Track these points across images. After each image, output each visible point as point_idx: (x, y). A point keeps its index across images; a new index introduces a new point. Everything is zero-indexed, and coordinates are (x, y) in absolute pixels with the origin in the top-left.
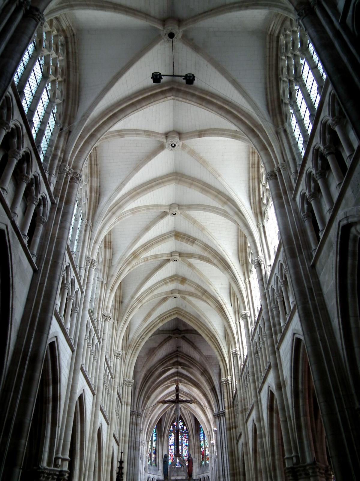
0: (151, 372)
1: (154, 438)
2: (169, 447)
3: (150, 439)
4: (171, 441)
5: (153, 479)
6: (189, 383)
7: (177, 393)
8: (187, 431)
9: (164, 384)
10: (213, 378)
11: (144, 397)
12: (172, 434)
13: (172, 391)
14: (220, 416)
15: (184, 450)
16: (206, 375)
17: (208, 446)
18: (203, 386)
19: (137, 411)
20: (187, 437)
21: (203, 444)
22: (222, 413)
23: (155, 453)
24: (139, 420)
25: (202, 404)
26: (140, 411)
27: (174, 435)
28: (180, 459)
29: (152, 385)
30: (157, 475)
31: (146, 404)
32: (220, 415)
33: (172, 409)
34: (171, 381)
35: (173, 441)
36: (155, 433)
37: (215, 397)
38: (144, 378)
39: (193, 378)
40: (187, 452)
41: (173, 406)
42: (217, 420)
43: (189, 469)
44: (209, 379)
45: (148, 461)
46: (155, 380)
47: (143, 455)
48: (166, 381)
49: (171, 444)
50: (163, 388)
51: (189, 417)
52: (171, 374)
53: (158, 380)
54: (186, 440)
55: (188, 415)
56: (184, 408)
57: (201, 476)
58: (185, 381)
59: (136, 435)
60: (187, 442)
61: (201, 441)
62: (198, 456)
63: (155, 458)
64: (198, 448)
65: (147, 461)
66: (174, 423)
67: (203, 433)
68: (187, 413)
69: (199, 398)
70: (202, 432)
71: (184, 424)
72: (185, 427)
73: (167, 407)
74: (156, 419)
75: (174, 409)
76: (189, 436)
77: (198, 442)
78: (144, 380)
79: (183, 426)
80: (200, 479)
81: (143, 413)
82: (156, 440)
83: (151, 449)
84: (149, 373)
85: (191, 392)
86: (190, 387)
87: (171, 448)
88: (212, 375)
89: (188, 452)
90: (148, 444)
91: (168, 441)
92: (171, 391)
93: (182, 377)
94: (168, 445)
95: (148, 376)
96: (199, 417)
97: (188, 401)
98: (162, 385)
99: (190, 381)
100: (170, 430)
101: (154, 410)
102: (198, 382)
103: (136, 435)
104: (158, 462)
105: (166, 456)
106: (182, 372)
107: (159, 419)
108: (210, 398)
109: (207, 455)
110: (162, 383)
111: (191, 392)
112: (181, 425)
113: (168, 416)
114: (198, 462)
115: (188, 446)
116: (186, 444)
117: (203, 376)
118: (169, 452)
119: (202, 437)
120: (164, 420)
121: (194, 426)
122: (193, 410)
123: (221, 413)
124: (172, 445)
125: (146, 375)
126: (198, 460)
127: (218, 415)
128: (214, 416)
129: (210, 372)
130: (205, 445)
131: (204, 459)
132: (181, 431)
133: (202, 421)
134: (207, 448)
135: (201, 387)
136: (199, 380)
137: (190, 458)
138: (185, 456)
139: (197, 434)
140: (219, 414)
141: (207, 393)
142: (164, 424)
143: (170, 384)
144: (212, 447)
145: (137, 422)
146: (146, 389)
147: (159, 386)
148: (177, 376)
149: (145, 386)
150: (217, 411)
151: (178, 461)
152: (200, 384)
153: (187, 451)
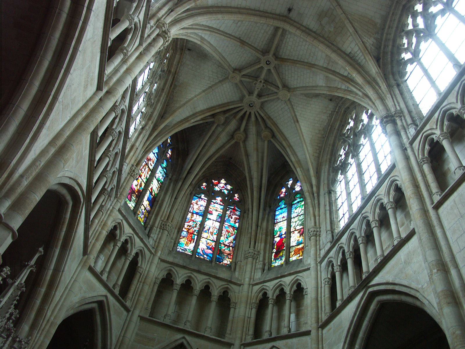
4: (196, 207)
15: (224, 232)
30: (141, 240)
35: (202, 208)
40: (231, 239)
49: (196, 210)
54: (234, 217)
60: (235, 222)
87: (193, 219)
89: (234, 239)
91: (189, 203)
94: (186, 211)
100: (200, 188)
115: (237, 229)
116: (232, 223)
118: (186, 224)
138: (225, 245)
142: (189, 163)
153: (233, 237)
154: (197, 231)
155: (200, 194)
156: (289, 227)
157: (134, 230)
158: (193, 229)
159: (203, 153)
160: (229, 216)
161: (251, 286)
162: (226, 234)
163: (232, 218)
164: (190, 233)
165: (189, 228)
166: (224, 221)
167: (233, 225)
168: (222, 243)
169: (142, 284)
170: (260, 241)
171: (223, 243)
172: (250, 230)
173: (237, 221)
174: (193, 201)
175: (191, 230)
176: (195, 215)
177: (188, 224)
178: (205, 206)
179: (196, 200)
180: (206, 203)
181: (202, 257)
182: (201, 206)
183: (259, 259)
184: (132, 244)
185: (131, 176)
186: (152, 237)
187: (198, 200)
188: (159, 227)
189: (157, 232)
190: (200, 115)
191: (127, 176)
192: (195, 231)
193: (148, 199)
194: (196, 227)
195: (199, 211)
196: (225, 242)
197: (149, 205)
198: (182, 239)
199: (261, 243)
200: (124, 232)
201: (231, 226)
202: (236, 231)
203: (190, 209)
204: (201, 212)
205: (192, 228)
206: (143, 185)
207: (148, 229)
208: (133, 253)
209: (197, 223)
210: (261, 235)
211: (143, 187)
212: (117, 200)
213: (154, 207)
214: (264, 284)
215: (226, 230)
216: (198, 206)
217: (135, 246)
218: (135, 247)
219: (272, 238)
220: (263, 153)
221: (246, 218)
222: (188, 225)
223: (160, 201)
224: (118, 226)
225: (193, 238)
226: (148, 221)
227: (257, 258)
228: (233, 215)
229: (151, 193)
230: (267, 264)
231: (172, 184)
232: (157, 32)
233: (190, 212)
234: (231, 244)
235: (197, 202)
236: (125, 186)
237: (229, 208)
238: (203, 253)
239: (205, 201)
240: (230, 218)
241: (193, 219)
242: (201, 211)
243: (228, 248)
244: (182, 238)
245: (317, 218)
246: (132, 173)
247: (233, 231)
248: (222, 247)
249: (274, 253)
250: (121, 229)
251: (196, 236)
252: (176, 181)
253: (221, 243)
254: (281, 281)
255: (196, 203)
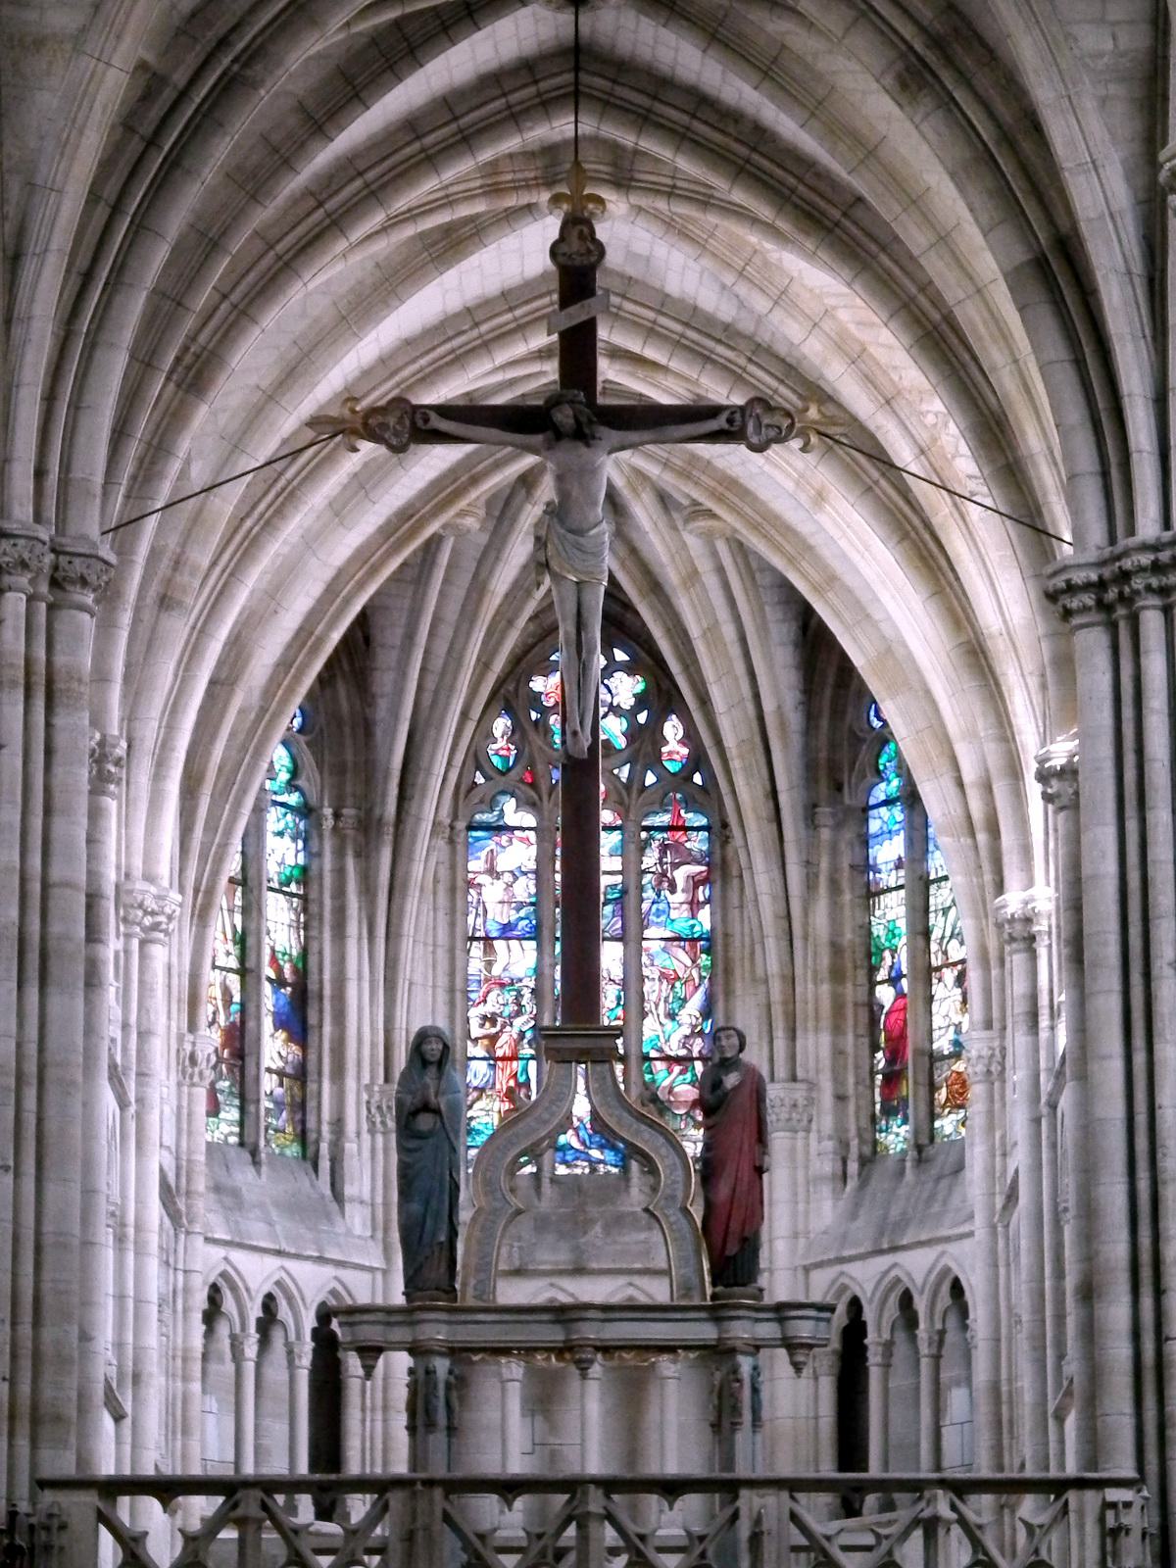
0: (223, 43)
1: (282, 853)
2: (477, 949)
3: (233, 865)
4: (493, 892)
5: (269, 1303)
6: (739, 196)
7: (577, 314)
8: (697, 779)
9: (402, 202)
10: (1059, 131)
11: (143, 361)
12: (509, 805)
13: (508, 298)
14: (1125, 600)
15: (653, 990)
16: (959, 95)
17: (956, 952)
18: (915, 238)
19: (45, 533)
20: (698, 843)
21: (902, 925)
22: (1157, 568)
23: (297, 1022)
24: (77, 637)
25: (903, 454)
26: (94, 532)
27: (529, 820)
28: (604, 1091)
29: (238, 216)
30: (321, 1260)
31: (158, 450)
32: (1138, 583)
33: (503, 511)
34: (493, 168)
35: (525, 889)
36: (293, 799)
37: (1079, 363)
38: (127, 124)
39: (787, 125)
41: (527, 482)
42: (1092, 644)
43: (723, 1191)
44: (1007, 139)
45: (214, 1110)
46: (282, 155)
47: (144, 1035)
48: (431, 160)
49: (499, 915)
50: (381, 247)
51: (723, 613)
52: (493, 82)
53: (324, 156)
54: (681, 875)
55: (711, 581)
56: (664, 499)
57: (865, 1277)
58: (688, 166)
59: (48, 811)
60: (694, 906)
61: (871, 894)
62: (838, 1052)
63: (299, 1075)
64: (837, 975)
65: (201, 1106)
66: (538, 684)
67: (910, 798)
68: (705, 566)
69: (869, 380)
70: (891, 786)
71: (661, 697)
72: (673, 728)
73: (436, 485)
74: (305, 636)
75: (531, 514)
76: (720, 831)
77: (835, 906)
78: (136, 146)
79: (642, 718)
80: (855, 1305)
81: (125, 551)
82: (304, 875)
83: (246, 971)
84: (191, 61)
85: (761, 304)
86: (753, 238)
88: (1043, 93)
89: (707, 1012)
90: (202, 915)
91: (458, 887)
92: (492, 287)
93: (644, 120)
95: (183, 95)
96: (862, 613)
97: (714, 411)
98: (378, 218)
99: (743, 171)
100: (477, 759)
101: (270, 524)
102: (859, 184)
103: (48, 811)
104: (338, 1124)
105: (433, 1048)
106: (645, 53)
107: (336, 636)
108: (1006, 382)
109: (942, 1043)
110: (375, 195)
111: (761, 304)
112: (626, 701)
113: (459, 593)
114: (826, 1122)
117: (927, 102)
118: (475, 1014)
119: (888, 852)
120: (410, 637)
121: (795, 719)
122: (788, 530)
123: (1146, 559)
124: (507, 931)
125: (149, 82)
126: (827, 1099)
127: (1101, 585)
128: (1052, 596)
129: (1026, 51)
130: (922, 932)
131: (907, 1088)
132: (624, 773)
133: (892, 652)
134: (949, 975)
135: (890, 244)
136: (868, 151)
137: (731, 1080)
138: (671, 1060)
139: (824, 810)
140: (1125, 576)
141: (969, 316)
143: (480, 207)
144: (1017, 961)
145: (60, 660)
146: (157, 257)
147: (337, 224)
148: (575, 98)
149: (141, 227)
150: (1097, 534)
151: (581, 1107)
152: (886, 207)
154: (529, 1035)
155: (491, 804)
156: (921, 942)
157: (279, 1253)
158: (508, 1028)
159: (437, 663)
160: (660, 883)
161: (800, 1275)
162: (664, 994)
163: (673, 889)
164: (503, 1059)
165: (494, 1030)
166: (643, 925)
167: (686, 932)
168: (653, 1054)
169: (379, 1416)
170: (811, 1024)
171: (660, 1050)
172: (760, 972)
173: (701, 899)
174: (473, 866)
175: (504, 1038)
176: (499, 945)
177: (482, 1010)
178: (532, 866)
179: (483, 854)
180: (533, 850)
181: (581, 1169)
182: (516, 878)
183: (819, 1123)
184: (290, 1299)
185: (193, 1085)
186: (352, 1200)
187: (491, 845)
188: (365, 1127)
189: (366, 1154)
190: (361, 585)
191: (179, 1098)
192: (522, 1035)
193: (280, 1023)
194: (519, 1013)
195: (514, 916)
196: (667, 1041)
197: (291, 1039)
198: (477, 1106)
199: (817, 1030)
200: (248, 1290)
201: (679, 939)
202: (704, 960)
203: (471, 919)
204: (522, 913)
205: (503, 1026)
206: (234, 982)
207: (325, 1164)
208: (309, 1322)
209: (519, 991)
210: (810, 986)
211: (237, 998)
212: (188, 1233)
213: (313, 1039)
214: (847, 1268)
215: (656, 975)
216: (500, 885)
217: (303, 1299)
218: (304, 1304)
219: (866, 988)
220: (720, 570)
221: (735, 882)
222: (485, 1018)
223: (327, 991)
224: (221, 1283)
225: (522, 1079)
226: (311, 1123)
227: (810, 1121)
228: (676, 866)
229: (279, 982)
230: (854, 1144)
231: (350, 863)
232: (135, 943)
233: (473, 939)
234: (698, 1045)
235: (491, 858)
236: (189, 1148)
237: (647, 829)
238: (583, 1143)
239: (522, 840)
240: (667, 893)
241: (496, 970)
242: (520, 906)
243: (682, 1072)
244: (474, 1102)
245: (995, 972)
246: (192, 1077)
247: (694, 962)
248: (659, 1077)
249: (880, 1077)
250: (234, 1288)
251: (533, 1064)
252: (368, 827)
253: (646, 1058)
254: (895, 1265)
255: (492, 872)
